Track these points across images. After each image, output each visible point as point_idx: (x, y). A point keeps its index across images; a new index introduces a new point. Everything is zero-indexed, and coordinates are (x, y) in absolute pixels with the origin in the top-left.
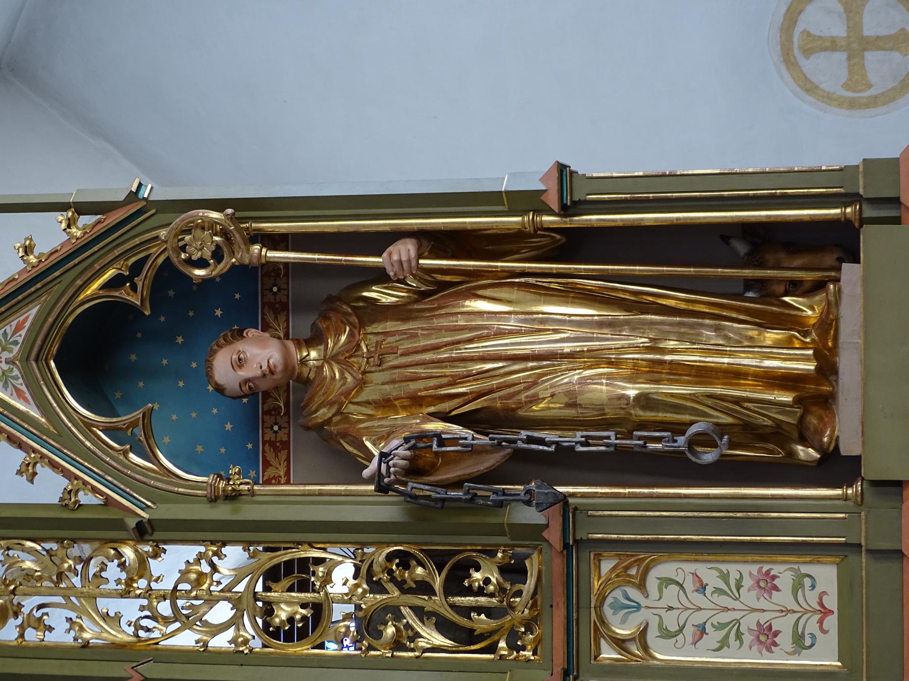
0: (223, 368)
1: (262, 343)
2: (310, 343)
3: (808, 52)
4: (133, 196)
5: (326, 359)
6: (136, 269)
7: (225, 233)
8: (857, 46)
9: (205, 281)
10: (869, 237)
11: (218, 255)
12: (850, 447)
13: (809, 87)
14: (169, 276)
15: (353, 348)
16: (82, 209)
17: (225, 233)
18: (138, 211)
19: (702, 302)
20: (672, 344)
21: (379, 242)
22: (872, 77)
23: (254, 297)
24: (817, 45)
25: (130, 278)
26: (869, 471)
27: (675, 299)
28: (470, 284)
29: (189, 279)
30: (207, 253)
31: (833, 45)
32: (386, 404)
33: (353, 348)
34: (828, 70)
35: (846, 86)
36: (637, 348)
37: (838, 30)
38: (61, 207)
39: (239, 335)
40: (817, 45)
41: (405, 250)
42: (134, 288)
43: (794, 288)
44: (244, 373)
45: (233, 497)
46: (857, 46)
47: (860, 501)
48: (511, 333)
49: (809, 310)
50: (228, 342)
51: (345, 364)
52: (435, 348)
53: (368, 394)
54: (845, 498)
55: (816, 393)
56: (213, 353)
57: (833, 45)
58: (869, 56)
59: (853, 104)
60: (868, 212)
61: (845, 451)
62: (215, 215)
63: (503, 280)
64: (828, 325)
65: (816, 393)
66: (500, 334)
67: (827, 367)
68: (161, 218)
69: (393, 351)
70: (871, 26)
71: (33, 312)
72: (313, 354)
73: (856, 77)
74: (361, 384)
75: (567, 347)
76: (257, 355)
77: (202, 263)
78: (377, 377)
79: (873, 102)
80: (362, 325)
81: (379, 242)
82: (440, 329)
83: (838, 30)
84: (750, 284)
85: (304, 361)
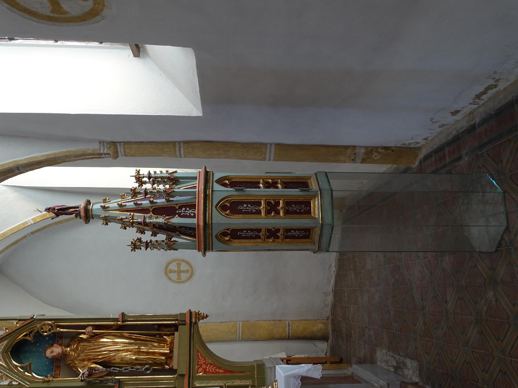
0: (48, 353)
1: (57, 348)
2: (68, 347)
3: (170, 273)
4: (32, 318)
5: (71, 350)
6: (31, 332)
7: (52, 326)
8: (179, 272)
9: (46, 335)
10: (180, 327)
11: (50, 330)
12: (175, 367)
13: (170, 279)
14: (38, 336)
15: (77, 348)
16: (19, 320)
17: (52, 326)
18: (33, 320)
19: (148, 338)
20: (143, 348)
21: (84, 327)
22: (182, 278)
23: (56, 338)
24: (172, 271)
25: (29, 334)
26: (179, 372)
27: (143, 337)
28: (102, 336)
29: (43, 335)
30: (47, 330)
31: (175, 271)
32: (83, 360)
33: (77, 348)
34: (174, 276)
35: (177, 279)
36: (136, 349)
37: (176, 269)
38: (16, 320)
39: (52, 345)
40: (172, 271)
41: (89, 329)
42: (30, 336)
43: (166, 335)
44: (53, 354)
45: (49, 381)
46: (179, 272)
47: (177, 378)
48: (111, 346)
49: (168, 339)
50: (50, 348)
51: (75, 352)
52: (95, 349)
53: (79, 358)
54: (174, 377)
55: (169, 357)
56: (46, 350)
57: (175, 271)
58: (182, 274)
59: (178, 282)
60: (180, 323)
61: (174, 368)
62: (50, 322)
63: (109, 335)
64: (172, 343)
65: (169, 357)
66: (108, 346)
67: (171, 351)
68: (37, 322)
69: (86, 349)
70: (182, 269)
71: (6, 342)
72: (68, 349)
73: (179, 277)
74: (78, 356)
75: (121, 349)
76: (57, 350)
77: (46, 332)
78: (82, 355)
79: (182, 282)
80: (79, 343)
81: (84, 327)
82: (96, 345)
83: (176, 269)
84: (157, 334)
85: (66, 351)
